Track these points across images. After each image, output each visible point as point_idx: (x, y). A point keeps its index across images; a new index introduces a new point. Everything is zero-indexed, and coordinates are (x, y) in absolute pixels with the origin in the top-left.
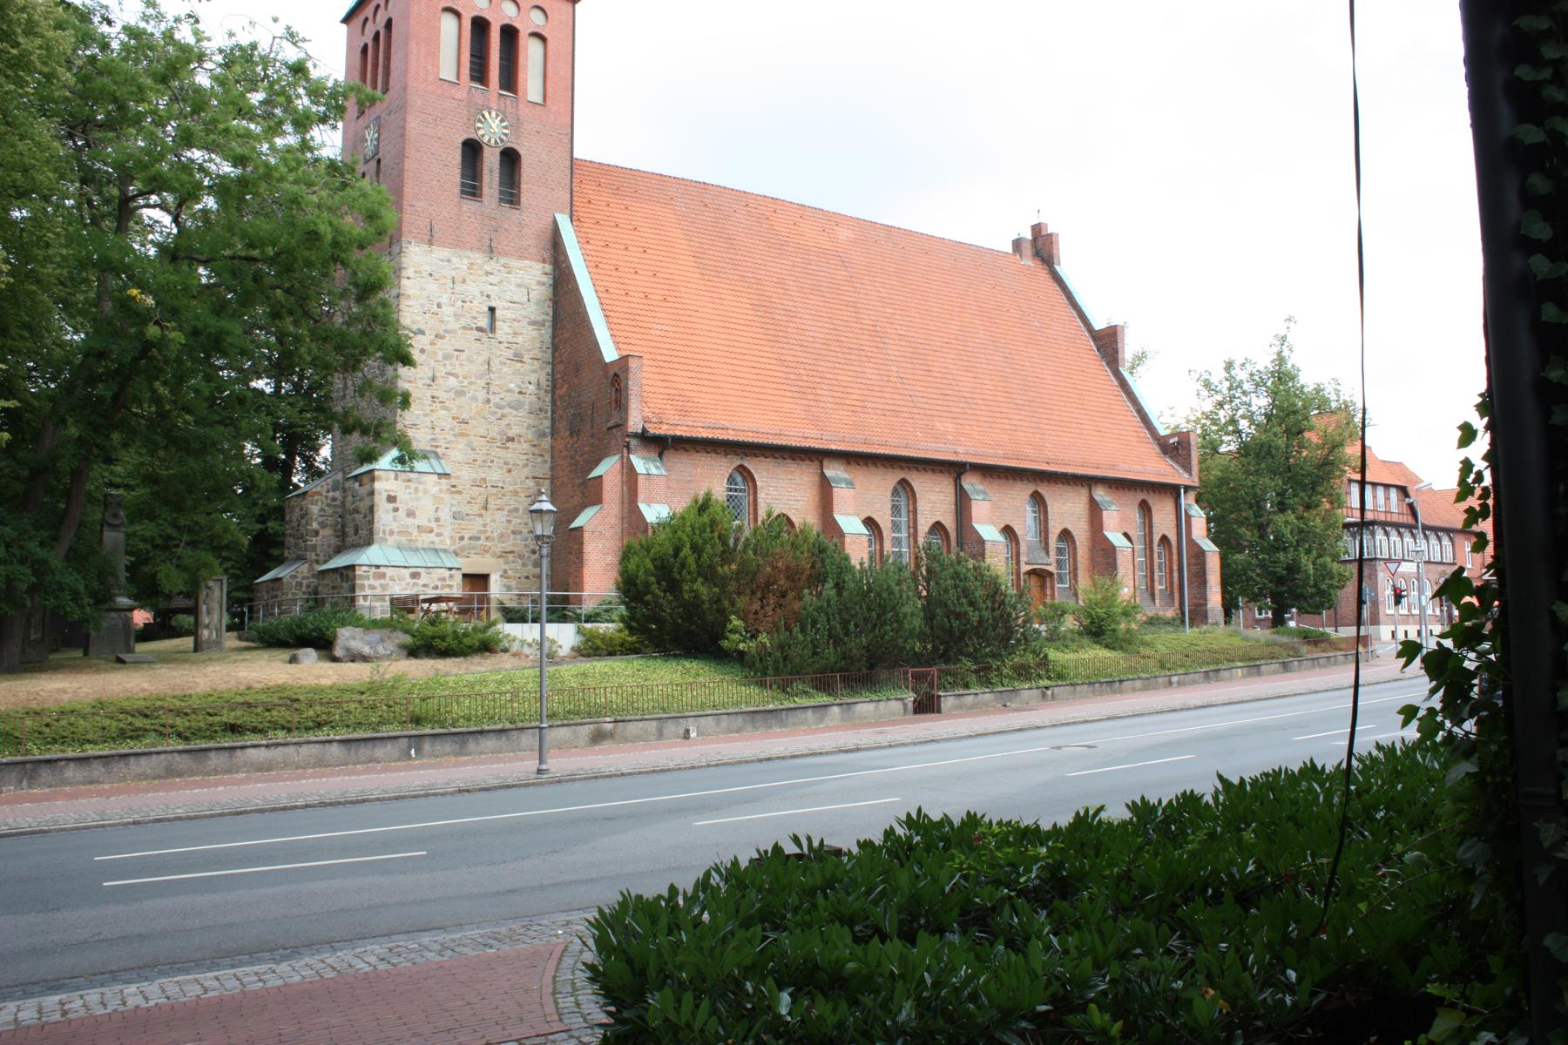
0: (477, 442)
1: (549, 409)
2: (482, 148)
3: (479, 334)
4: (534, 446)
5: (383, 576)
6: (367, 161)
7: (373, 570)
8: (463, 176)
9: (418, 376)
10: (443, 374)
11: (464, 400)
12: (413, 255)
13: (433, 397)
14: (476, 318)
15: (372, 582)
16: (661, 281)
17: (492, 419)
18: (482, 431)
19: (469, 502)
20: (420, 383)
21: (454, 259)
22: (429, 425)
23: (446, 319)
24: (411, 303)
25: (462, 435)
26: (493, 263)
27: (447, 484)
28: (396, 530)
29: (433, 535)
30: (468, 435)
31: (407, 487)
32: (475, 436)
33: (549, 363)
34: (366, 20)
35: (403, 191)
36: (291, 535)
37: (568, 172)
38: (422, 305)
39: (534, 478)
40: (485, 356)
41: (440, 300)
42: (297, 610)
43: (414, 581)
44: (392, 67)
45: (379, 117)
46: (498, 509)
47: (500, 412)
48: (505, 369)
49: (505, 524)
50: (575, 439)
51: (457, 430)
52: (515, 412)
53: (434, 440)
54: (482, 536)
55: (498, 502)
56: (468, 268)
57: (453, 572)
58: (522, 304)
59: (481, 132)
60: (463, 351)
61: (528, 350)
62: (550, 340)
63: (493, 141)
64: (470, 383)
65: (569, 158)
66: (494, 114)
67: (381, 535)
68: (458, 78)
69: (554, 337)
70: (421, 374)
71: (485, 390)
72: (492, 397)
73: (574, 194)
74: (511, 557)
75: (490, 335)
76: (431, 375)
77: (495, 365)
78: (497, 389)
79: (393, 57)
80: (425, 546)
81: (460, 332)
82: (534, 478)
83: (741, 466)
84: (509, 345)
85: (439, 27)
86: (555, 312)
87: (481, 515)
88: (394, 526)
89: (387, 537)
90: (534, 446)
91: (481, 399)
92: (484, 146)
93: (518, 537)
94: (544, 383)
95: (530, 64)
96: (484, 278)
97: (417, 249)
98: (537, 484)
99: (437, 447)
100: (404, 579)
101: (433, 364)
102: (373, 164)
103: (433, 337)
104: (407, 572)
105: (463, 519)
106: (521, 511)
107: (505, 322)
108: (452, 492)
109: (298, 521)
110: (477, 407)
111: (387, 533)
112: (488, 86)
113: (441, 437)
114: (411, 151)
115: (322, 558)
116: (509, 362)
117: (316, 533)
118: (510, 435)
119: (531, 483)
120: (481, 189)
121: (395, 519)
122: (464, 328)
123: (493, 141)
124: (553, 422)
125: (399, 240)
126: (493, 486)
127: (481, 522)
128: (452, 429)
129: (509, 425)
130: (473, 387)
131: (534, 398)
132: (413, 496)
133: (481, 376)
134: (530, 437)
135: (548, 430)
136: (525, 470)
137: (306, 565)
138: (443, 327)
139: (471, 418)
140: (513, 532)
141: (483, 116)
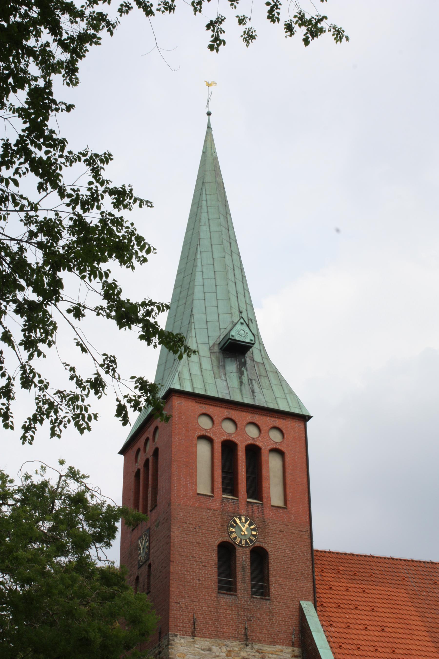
2: (235, 548)
6: (140, 567)
8: (220, 574)
12: (179, 646)
26: (248, 649)
34: (139, 450)
35: (169, 590)
37: (309, 563)
45: (150, 528)
56: (227, 656)
59: (234, 535)
63: (243, 542)
65: (309, 551)
66: (243, 519)
68: (212, 491)
73: (317, 582)
79: (159, 478)
85: (196, 452)
92: (237, 547)
95: (271, 474)
102: (145, 568)
112: (237, 497)
120: (236, 585)
123: (243, 542)
125: (167, 634)
141: (235, 522)
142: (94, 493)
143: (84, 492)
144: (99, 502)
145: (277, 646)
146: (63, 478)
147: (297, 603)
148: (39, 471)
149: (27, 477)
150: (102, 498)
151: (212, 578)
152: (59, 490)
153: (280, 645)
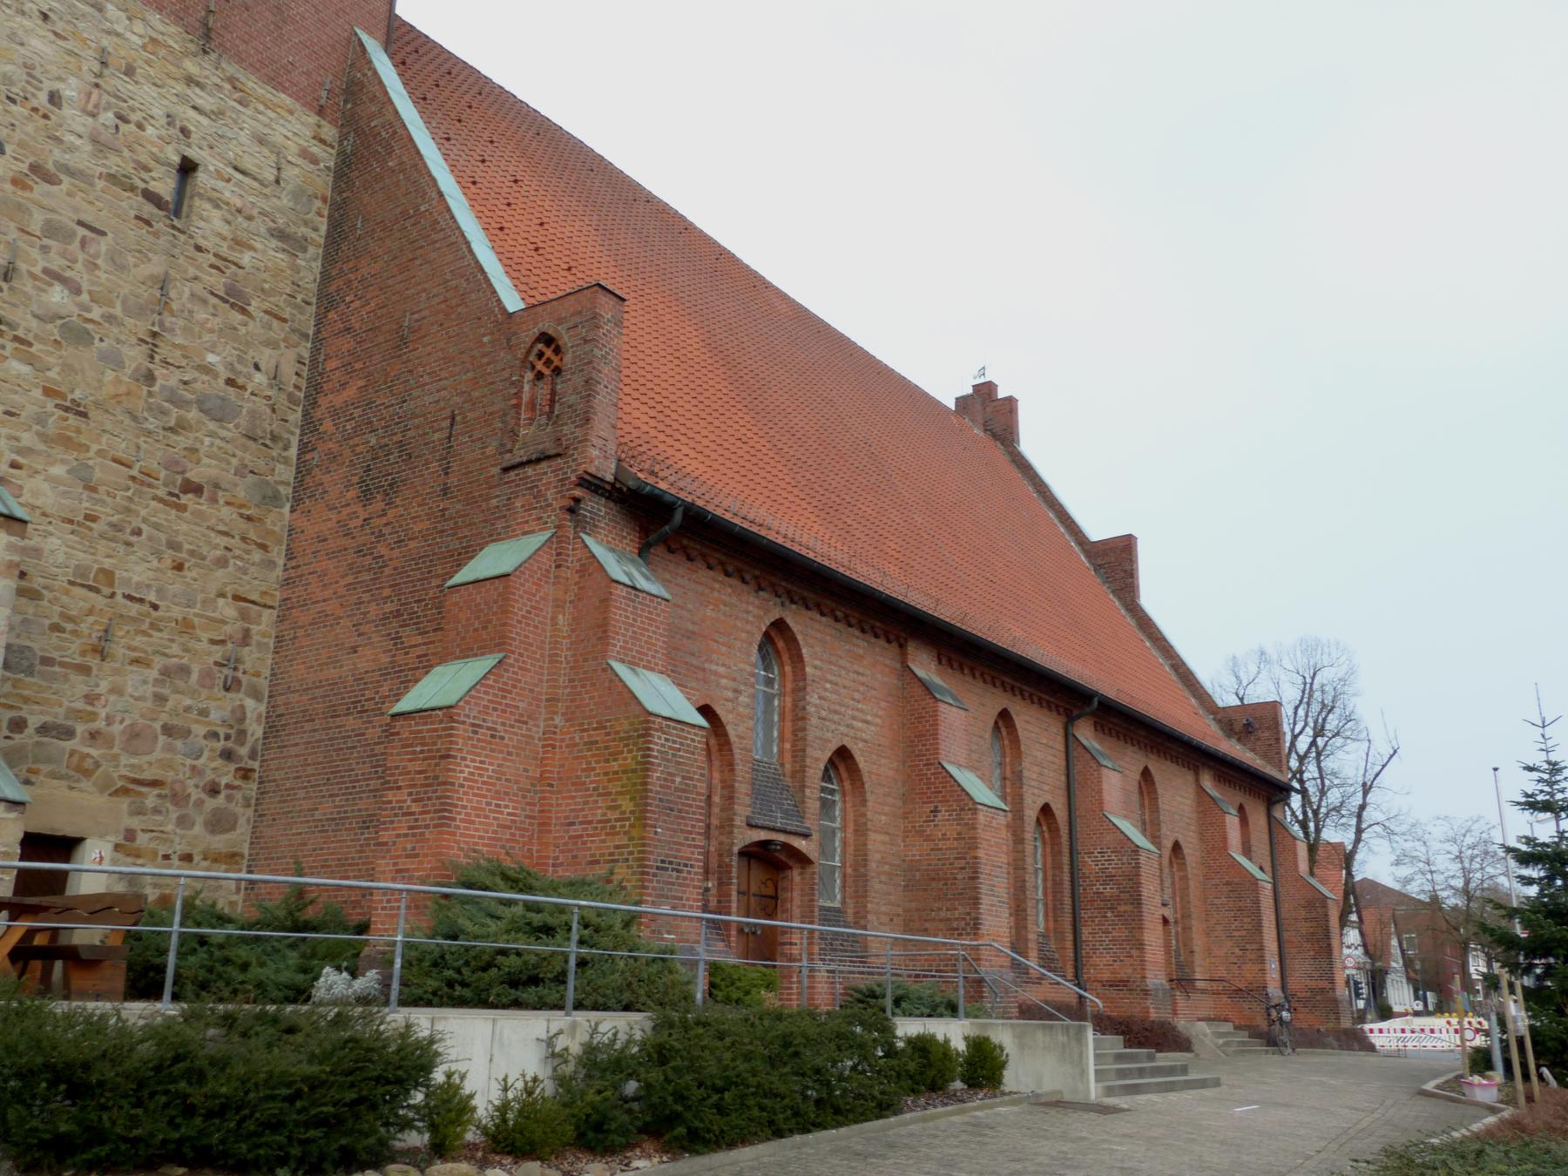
0: (102, 471)
3: (149, 209)
4: (249, 518)
17: (152, 424)
18: (122, 448)
19: (56, 628)
25: (66, 442)
26: (207, 62)
39: (237, 598)
40: (156, 266)
46: (136, 661)
48: (201, 315)
49: (149, 704)
50: (382, 505)
51: (52, 426)
52: (212, 426)
54: (80, 729)
55: (139, 641)
58: (262, 184)
60: (103, 234)
69: (325, 278)
72: (159, 372)
74: (151, 798)
77: (181, 294)
78: (176, 357)
81: (100, 184)
82: (237, 598)
83: (779, 626)
84: (220, 263)
87: (85, 670)
90: (249, 518)
93: (179, 744)
96: (180, 87)
98: (244, 616)
103: (24, 168)
105: (30, 671)
106: (195, 676)
107: (217, 207)
110: (118, 381)
118: (194, 475)
122: (112, 178)
124: (303, 470)
126: (129, 597)
127: (84, 689)
128: (40, 420)
129: (194, 451)
131: (261, 405)
133: (140, 312)
136: (220, 573)
139: (97, 404)
140: (168, 730)
145: (283, 96)
153: (291, 96)
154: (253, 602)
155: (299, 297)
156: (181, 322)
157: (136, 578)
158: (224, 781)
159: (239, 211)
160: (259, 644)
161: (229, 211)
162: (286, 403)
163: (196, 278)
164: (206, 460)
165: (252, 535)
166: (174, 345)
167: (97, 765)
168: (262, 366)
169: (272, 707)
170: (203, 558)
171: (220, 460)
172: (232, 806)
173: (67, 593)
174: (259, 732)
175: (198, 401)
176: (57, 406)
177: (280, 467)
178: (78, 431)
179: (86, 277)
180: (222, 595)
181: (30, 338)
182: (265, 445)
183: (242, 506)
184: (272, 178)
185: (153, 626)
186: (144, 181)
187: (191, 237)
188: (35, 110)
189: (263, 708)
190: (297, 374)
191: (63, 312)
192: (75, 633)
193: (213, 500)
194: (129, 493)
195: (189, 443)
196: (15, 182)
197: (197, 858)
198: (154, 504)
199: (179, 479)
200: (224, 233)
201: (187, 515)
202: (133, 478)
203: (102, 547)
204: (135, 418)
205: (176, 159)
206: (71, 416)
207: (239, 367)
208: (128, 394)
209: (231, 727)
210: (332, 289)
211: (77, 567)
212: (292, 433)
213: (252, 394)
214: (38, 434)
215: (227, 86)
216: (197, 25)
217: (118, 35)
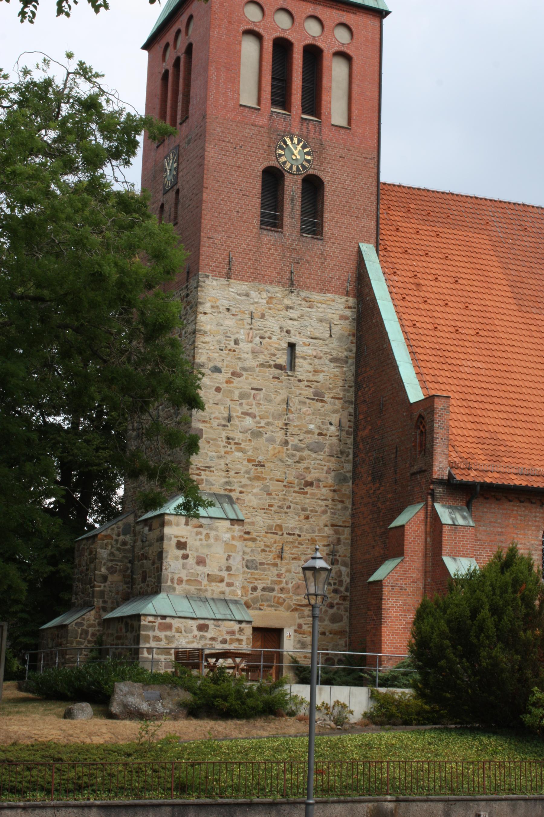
0: (274, 486)
1: (351, 451)
4: (334, 491)
5: (169, 627)
6: (166, 192)
7: (159, 620)
9: (213, 416)
10: (239, 414)
11: (262, 441)
13: (228, 438)
14: (274, 355)
15: (157, 633)
16: (473, 313)
17: (290, 461)
18: (279, 475)
19: (263, 551)
20: (215, 423)
21: (253, 294)
22: (223, 467)
23: (243, 356)
24: (207, 339)
25: (258, 478)
26: (293, 296)
27: (240, 530)
28: (185, 579)
29: (224, 584)
30: (264, 479)
31: (198, 533)
32: (271, 479)
33: (351, 403)
34: (167, 45)
35: (201, 222)
36: (79, 580)
38: (219, 342)
39: (333, 525)
41: (237, 336)
42: (80, 661)
43: (201, 633)
44: (192, 94)
46: (294, 559)
47: (298, 454)
48: (304, 409)
50: (377, 485)
51: (252, 474)
52: (314, 455)
53: (227, 483)
54: (277, 587)
55: (294, 550)
57: (243, 625)
58: (324, 340)
59: (282, 159)
60: (261, 390)
61: (330, 389)
62: (353, 378)
63: (294, 169)
64: (268, 424)
65: (374, 183)
66: (296, 140)
67: (169, 583)
68: (259, 103)
69: (357, 375)
70: (217, 414)
71: (283, 431)
72: (290, 439)
73: (381, 221)
75: (290, 373)
76: (226, 415)
77: (294, 405)
78: (295, 431)
79: (192, 83)
80: (215, 596)
81: (258, 369)
82: (333, 525)
84: (309, 384)
86: (358, 348)
87: (276, 565)
88: (184, 575)
89: (175, 585)
90: (334, 491)
91: (278, 441)
92: (286, 174)
94: (346, 424)
95: (334, 85)
96: (283, 313)
97: (215, 283)
98: (337, 532)
99: (231, 490)
100: (191, 632)
101: (229, 403)
103: (229, 375)
104: (194, 624)
105: (256, 568)
107: (305, 359)
108: (245, 540)
109: (87, 565)
110: (275, 448)
111: (176, 581)
113: (236, 480)
114: (209, 181)
115: (109, 605)
116: (308, 401)
117: (105, 578)
118: (309, 479)
119: (328, 531)
120: (282, 220)
121: (184, 566)
122: (262, 365)
123: (294, 169)
124: (355, 466)
125: (196, 275)
126: (289, 534)
127: (276, 572)
128: (247, 472)
129: (308, 468)
130: (270, 428)
131: (335, 440)
132: (204, 542)
133: (280, 416)
134: (330, 481)
135: (349, 475)
136: (324, 517)
137: (93, 612)
138: (240, 364)
139: (267, 460)
142: (110, 97)
143: (98, 95)
144: (117, 109)
145: (328, 295)
146: (71, 76)
147: (356, 245)
148: (41, 65)
149: (26, 72)
150: (121, 105)
151: (253, 210)
152: (67, 91)
153: (332, 293)
154: (340, 526)
155: (347, 386)
156: (297, 415)
157: (291, 526)
158: (335, 602)
159: (315, 357)
160: (344, 543)
161: (311, 359)
162: (346, 435)
163: (300, 394)
164: (313, 471)
165: (336, 498)
166: (295, 426)
167: (284, 600)
168: (333, 422)
169: (352, 570)
170: (317, 512)
171: (318, 469)
172: (340, 612)
173: (266, 537)
174: (348, 580)
175: (307, 447)
176: (253, 465)
177: (346, 465)
178: (262, 473)
179: (257, 410)
180: (326, 526)
181: (240, 442)
182: (338, 457)
183: (330, 486)
184: (328, 335)
185: (299, 543)
186: (274, 361)
187: (296, 377)
188: (230, 350)
189: (349, 570)
190: (349, 421)
191: (250, 427)
192: (270, 551)
193: (318, 487)
194: (284, 492)
195: (305, 465)
196: (227, 382)
197: (327, 634)
198: (294, 494)
199: (303, 481)
200: (309, 369)
201: (308, 496)
202: (285, 486)
203: (276, 516)
204: (282, 461)
205: (286, 345)
206: (258, 468)
207: (322, 427)
208: (279, 452)
209: (336, 579)
210: (359, 380)
211: (268, 526)
212: (350, 448)
213: (330, 436)
214: (248, 478)
215: (304, 302)
216: (287, 282)
217: (256, 303)
